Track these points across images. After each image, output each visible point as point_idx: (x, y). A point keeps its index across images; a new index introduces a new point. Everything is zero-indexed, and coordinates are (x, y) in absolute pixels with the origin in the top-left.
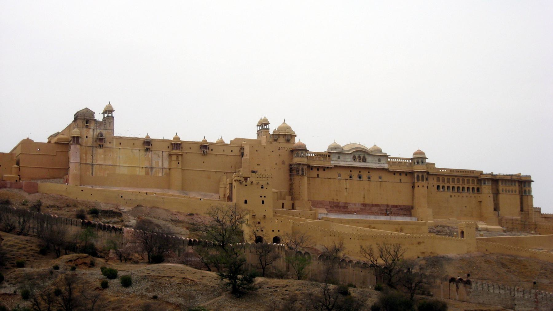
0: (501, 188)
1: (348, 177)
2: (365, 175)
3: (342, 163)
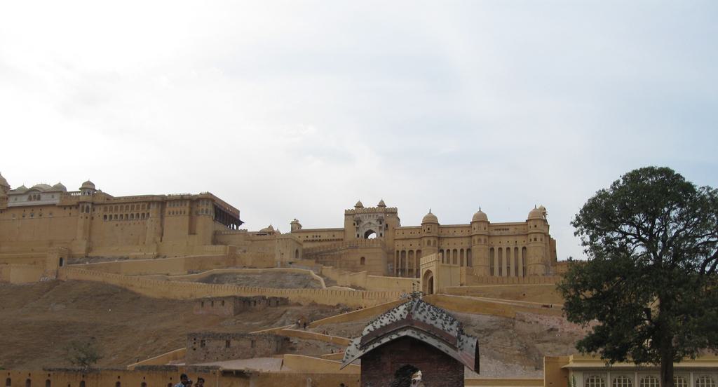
0: (167, 210)
1: (21, 217)
2: (37, 212)
3: (18, 204)
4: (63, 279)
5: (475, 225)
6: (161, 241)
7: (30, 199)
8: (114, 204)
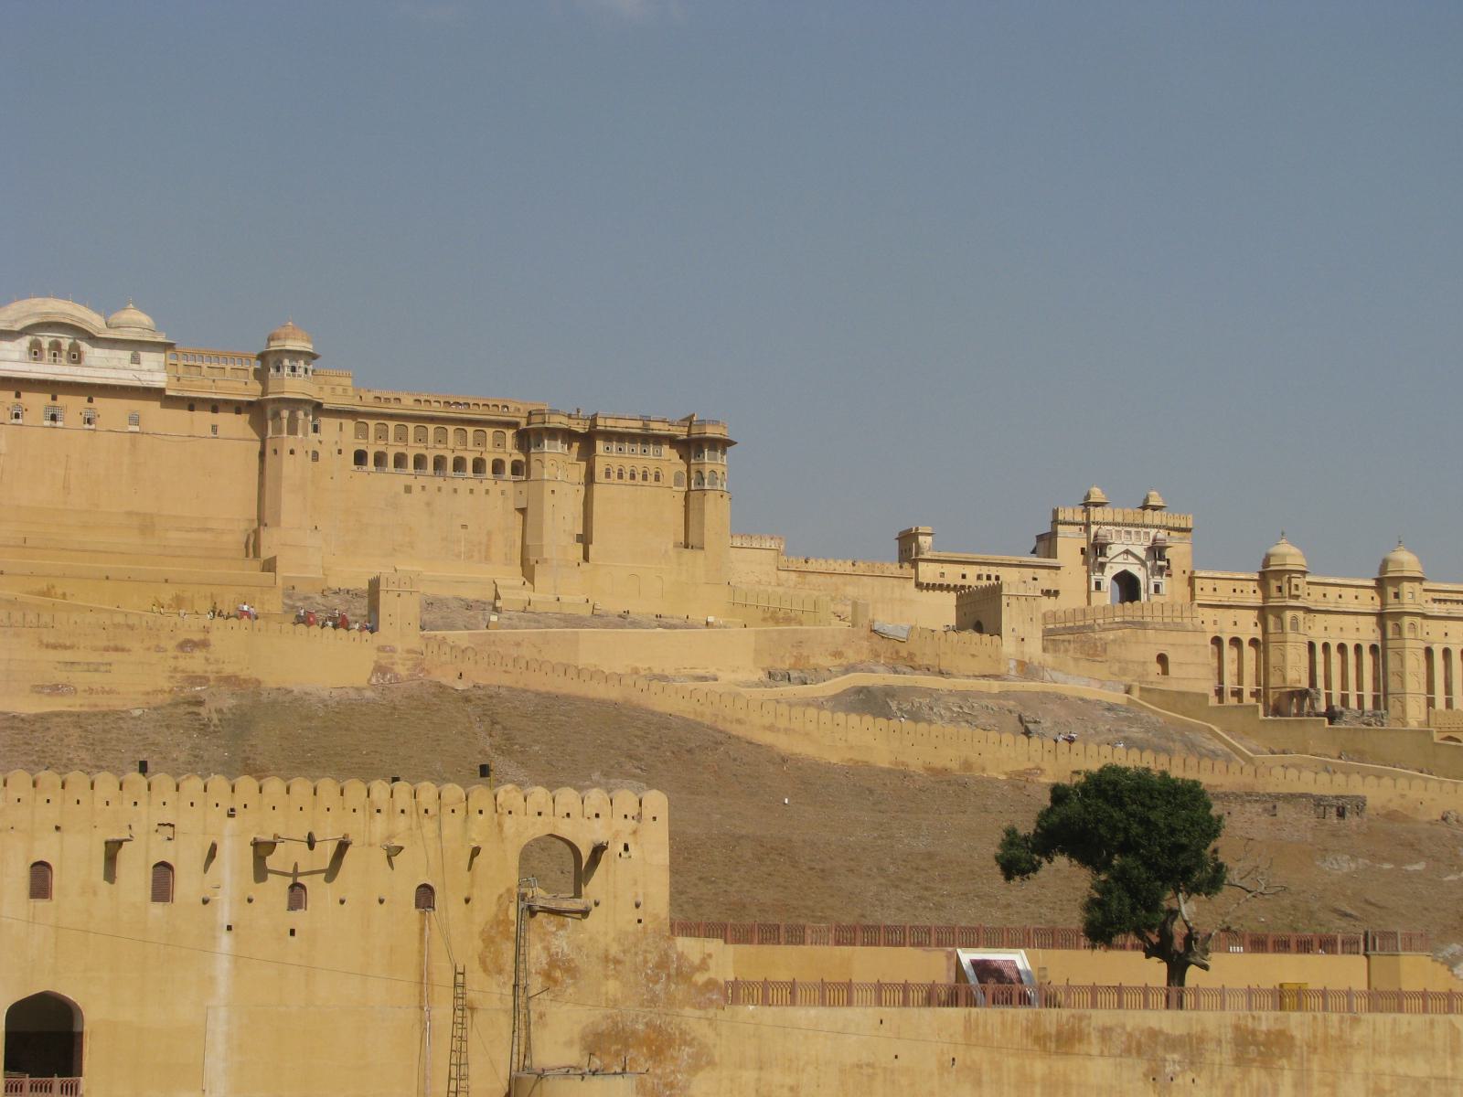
2: (73, 406)
5: (1406, 587)
6: (586, 558)
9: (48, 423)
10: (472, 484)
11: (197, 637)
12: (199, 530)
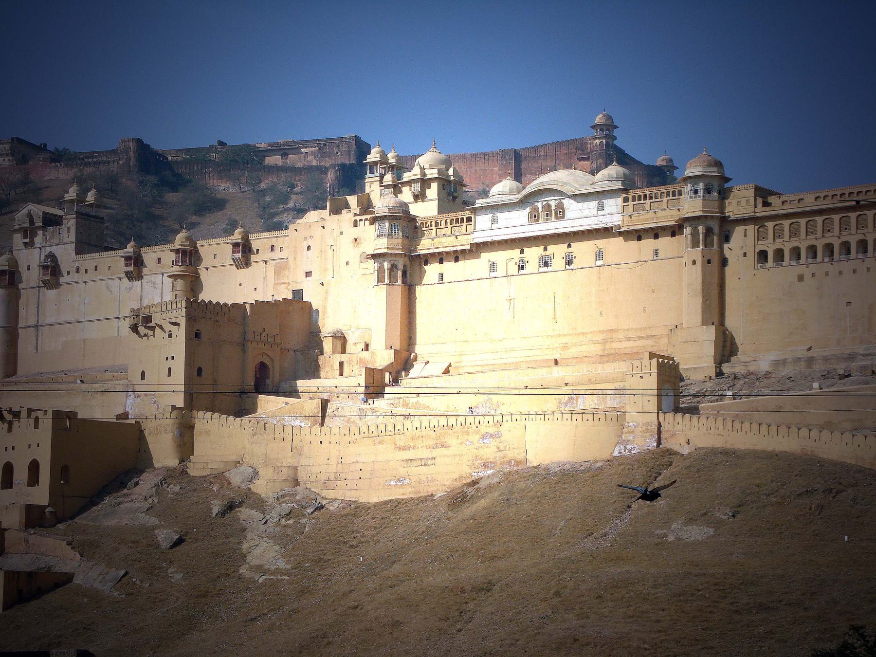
1: (513, 269)
2: (558, 251)
4: (676, 448)
7: (534, 217)
8: (787, 216)
9: (543, 269)
10: (827, 266)
11: (492, 430)
12: (643, 338)
